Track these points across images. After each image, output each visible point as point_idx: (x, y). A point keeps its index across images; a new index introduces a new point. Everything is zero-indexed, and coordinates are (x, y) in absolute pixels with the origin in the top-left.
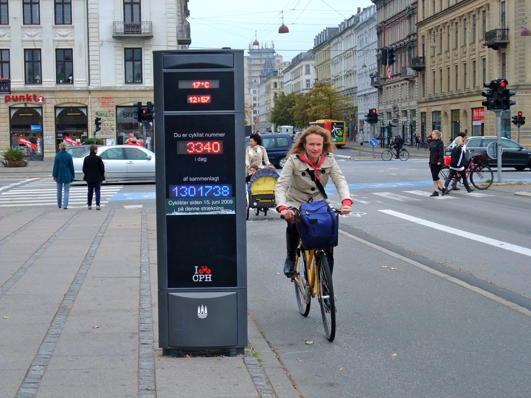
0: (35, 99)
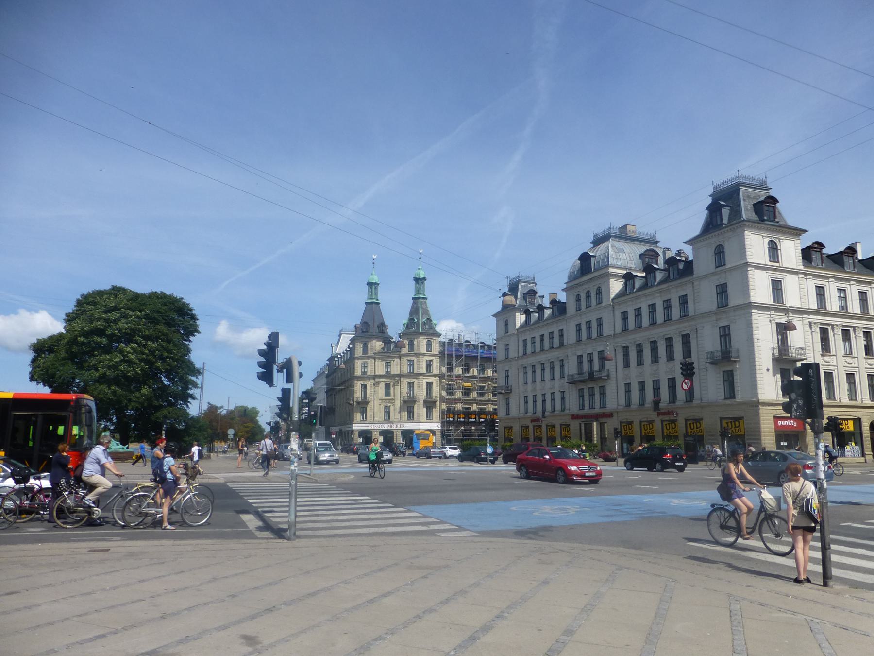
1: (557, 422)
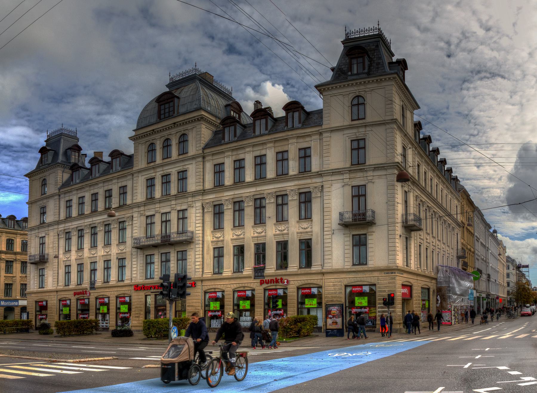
0: (282, 282)
1: (112, 294)
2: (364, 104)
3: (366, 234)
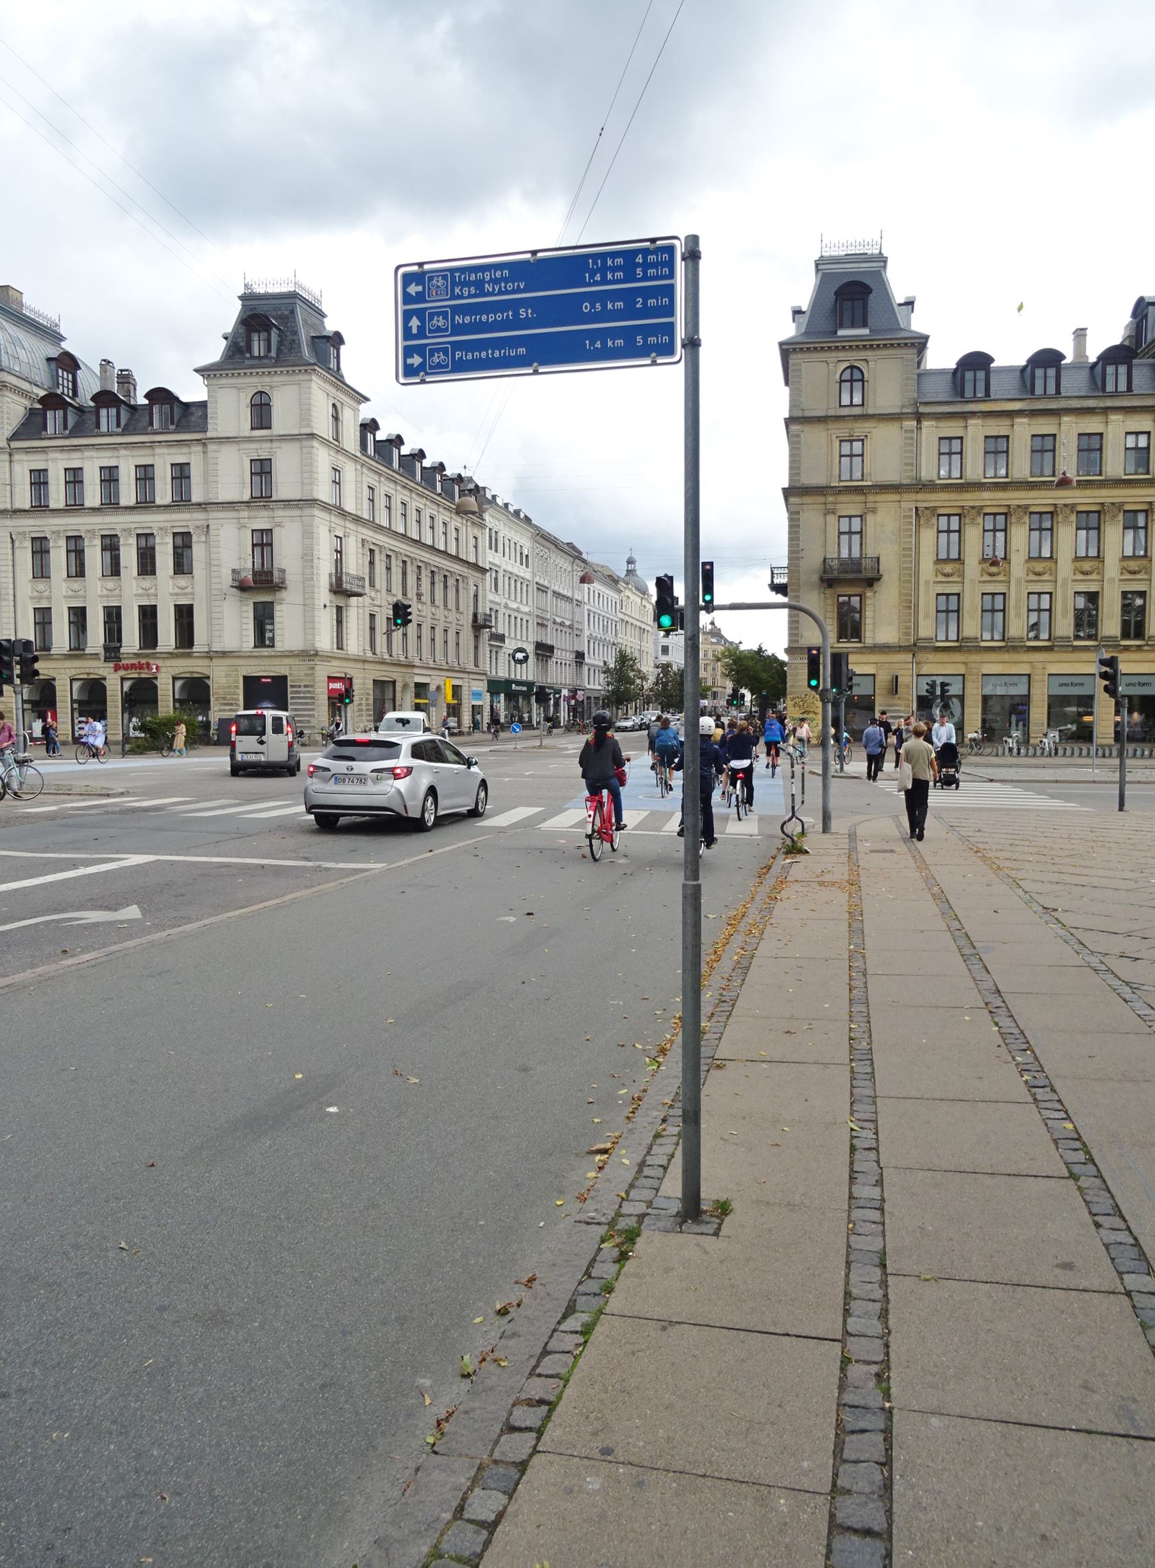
2: (269, 404)
3: (272, 603)
